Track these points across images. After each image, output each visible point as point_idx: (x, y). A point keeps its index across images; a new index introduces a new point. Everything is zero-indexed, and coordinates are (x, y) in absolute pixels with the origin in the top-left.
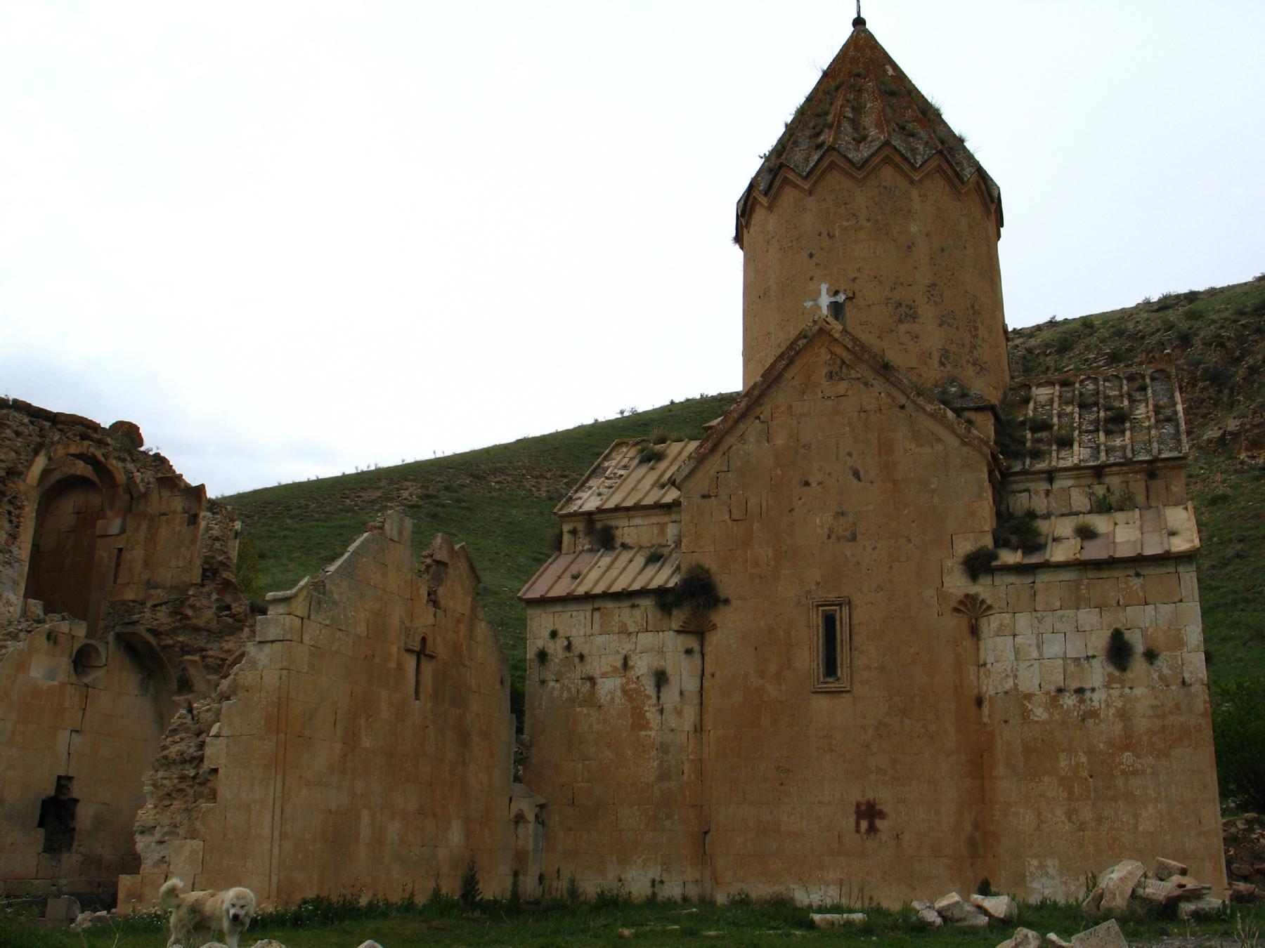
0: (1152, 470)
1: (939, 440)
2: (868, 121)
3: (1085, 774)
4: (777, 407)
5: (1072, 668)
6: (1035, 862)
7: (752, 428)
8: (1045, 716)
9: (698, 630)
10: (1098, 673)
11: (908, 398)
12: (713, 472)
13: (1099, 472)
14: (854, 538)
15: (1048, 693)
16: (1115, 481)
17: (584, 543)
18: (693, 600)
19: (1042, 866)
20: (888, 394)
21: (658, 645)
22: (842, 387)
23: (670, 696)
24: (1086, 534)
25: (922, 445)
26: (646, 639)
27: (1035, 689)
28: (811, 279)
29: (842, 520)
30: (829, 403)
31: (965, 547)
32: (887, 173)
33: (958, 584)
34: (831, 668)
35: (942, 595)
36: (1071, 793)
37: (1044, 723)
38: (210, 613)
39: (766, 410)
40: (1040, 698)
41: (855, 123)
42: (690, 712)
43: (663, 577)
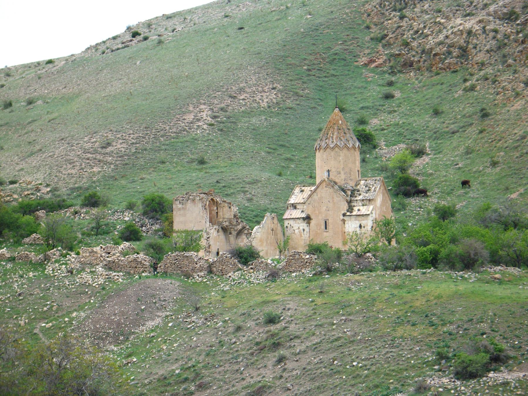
0: (370, 200)
2: (335, 137)
7: (315, 194)
9: (309, 223)
10: (358, 229)
13: (363, 200)
16: (365, 201)
17: (292, 208)
18: (308, 219)
21: (303, 225)
23: (305, 232)
24: (359, 210)
26: (302, 224)
31: (343, 212)
32: (336, 149)
33: (342, 217)
34: (326, 228)
38: (235, 223)
39: (317, 191)
41: (332, 137)
42: (308, 234)
43: (304, 215)
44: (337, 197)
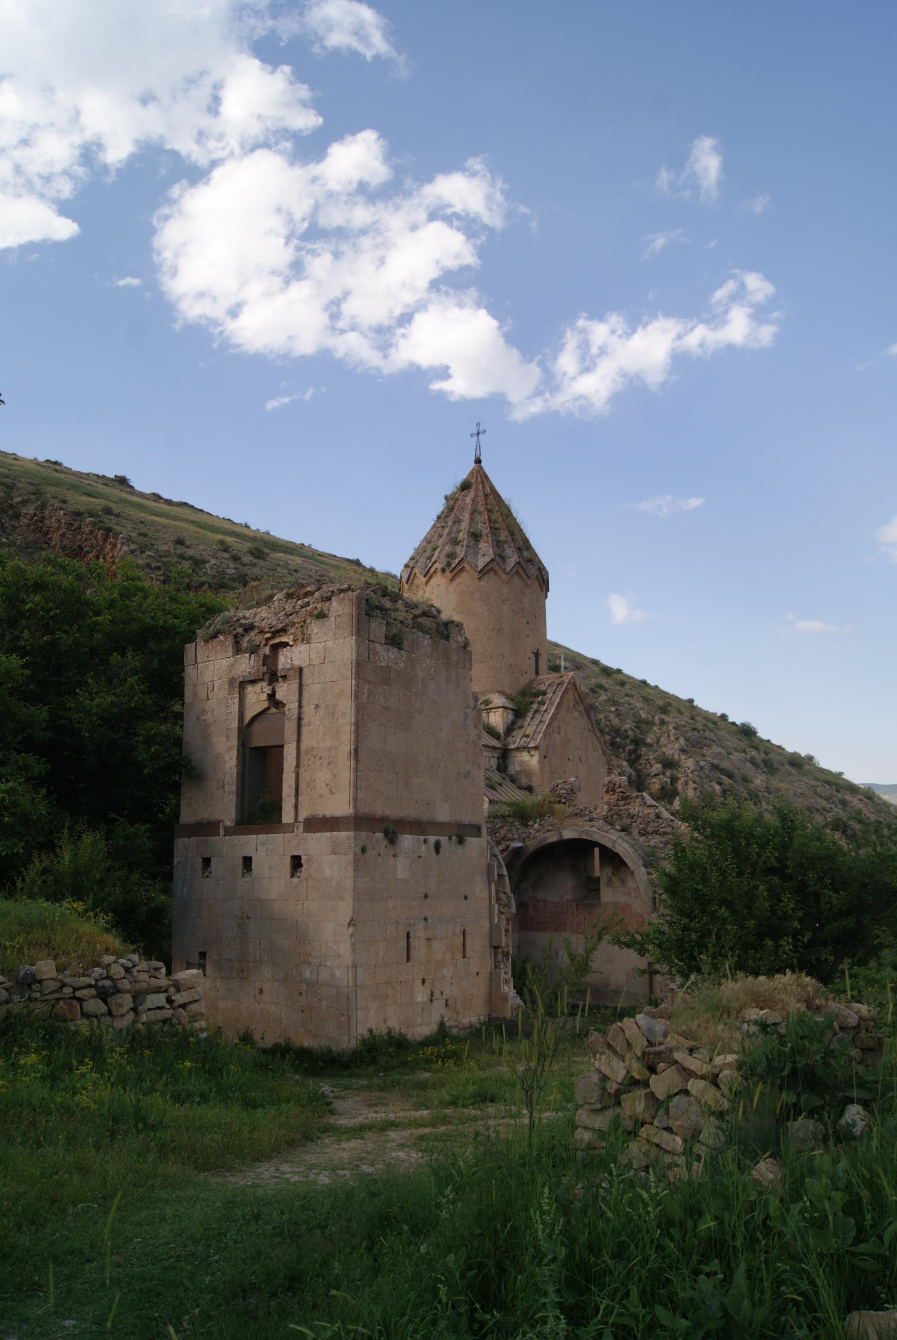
22: (576, 714)
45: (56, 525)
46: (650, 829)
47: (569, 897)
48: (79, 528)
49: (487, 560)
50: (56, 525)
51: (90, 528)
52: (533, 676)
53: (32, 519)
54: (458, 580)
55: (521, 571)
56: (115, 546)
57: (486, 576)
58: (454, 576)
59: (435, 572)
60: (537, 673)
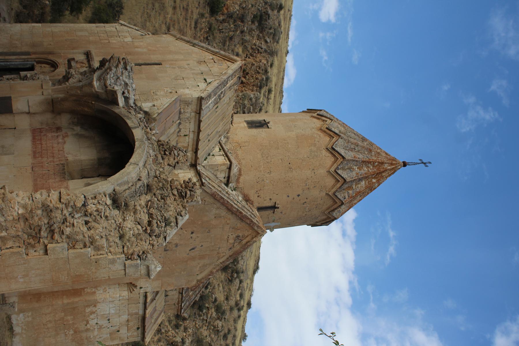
1: (201, 272)
3: (65, 323)
4: (229, 219)
5: (106, 316)
6: (30, 314)
8: (87, 311)
11: (221, 263)
12: (205, 199)
14: (165, 250)
15: (96, 311)
19: (28, 317)
20: (224, 256)
22: (231, 241)
25: (200, 267)
27: (98, 307)
28: (288, 196)
29: (174, 246)
30: (226, 237)
35: (137, 279)
36: (58, 321)
37: (85, 311)
40: (94, 309)
44: (205, 266)
45: (258, 60)
46: (152, 211)
47: (70, 158)
48: (259, 73)
49: (343, 154)
50: (258, 60)
51: (260, 78)
52: (256, 205)
53: (259, 47)
54: (322, 135)
55: (339, 185)
56: (252, 91)
57: (330, 155)
58: (325, 132)
59: (323, 121)
60: (260, 209)
